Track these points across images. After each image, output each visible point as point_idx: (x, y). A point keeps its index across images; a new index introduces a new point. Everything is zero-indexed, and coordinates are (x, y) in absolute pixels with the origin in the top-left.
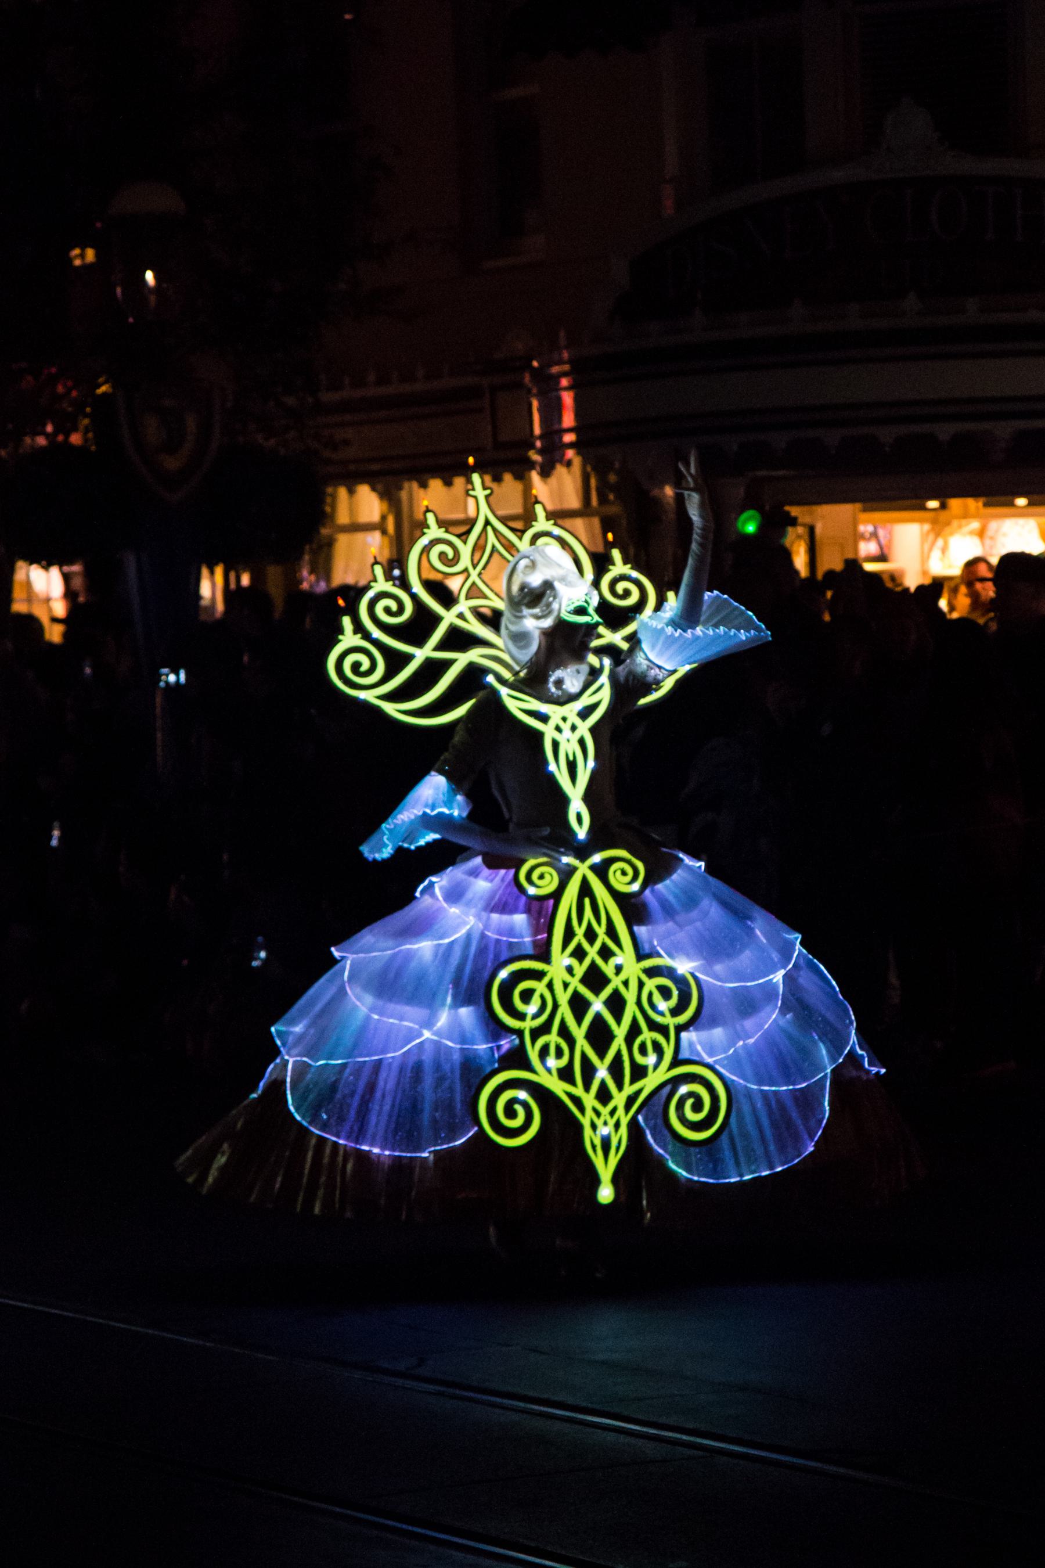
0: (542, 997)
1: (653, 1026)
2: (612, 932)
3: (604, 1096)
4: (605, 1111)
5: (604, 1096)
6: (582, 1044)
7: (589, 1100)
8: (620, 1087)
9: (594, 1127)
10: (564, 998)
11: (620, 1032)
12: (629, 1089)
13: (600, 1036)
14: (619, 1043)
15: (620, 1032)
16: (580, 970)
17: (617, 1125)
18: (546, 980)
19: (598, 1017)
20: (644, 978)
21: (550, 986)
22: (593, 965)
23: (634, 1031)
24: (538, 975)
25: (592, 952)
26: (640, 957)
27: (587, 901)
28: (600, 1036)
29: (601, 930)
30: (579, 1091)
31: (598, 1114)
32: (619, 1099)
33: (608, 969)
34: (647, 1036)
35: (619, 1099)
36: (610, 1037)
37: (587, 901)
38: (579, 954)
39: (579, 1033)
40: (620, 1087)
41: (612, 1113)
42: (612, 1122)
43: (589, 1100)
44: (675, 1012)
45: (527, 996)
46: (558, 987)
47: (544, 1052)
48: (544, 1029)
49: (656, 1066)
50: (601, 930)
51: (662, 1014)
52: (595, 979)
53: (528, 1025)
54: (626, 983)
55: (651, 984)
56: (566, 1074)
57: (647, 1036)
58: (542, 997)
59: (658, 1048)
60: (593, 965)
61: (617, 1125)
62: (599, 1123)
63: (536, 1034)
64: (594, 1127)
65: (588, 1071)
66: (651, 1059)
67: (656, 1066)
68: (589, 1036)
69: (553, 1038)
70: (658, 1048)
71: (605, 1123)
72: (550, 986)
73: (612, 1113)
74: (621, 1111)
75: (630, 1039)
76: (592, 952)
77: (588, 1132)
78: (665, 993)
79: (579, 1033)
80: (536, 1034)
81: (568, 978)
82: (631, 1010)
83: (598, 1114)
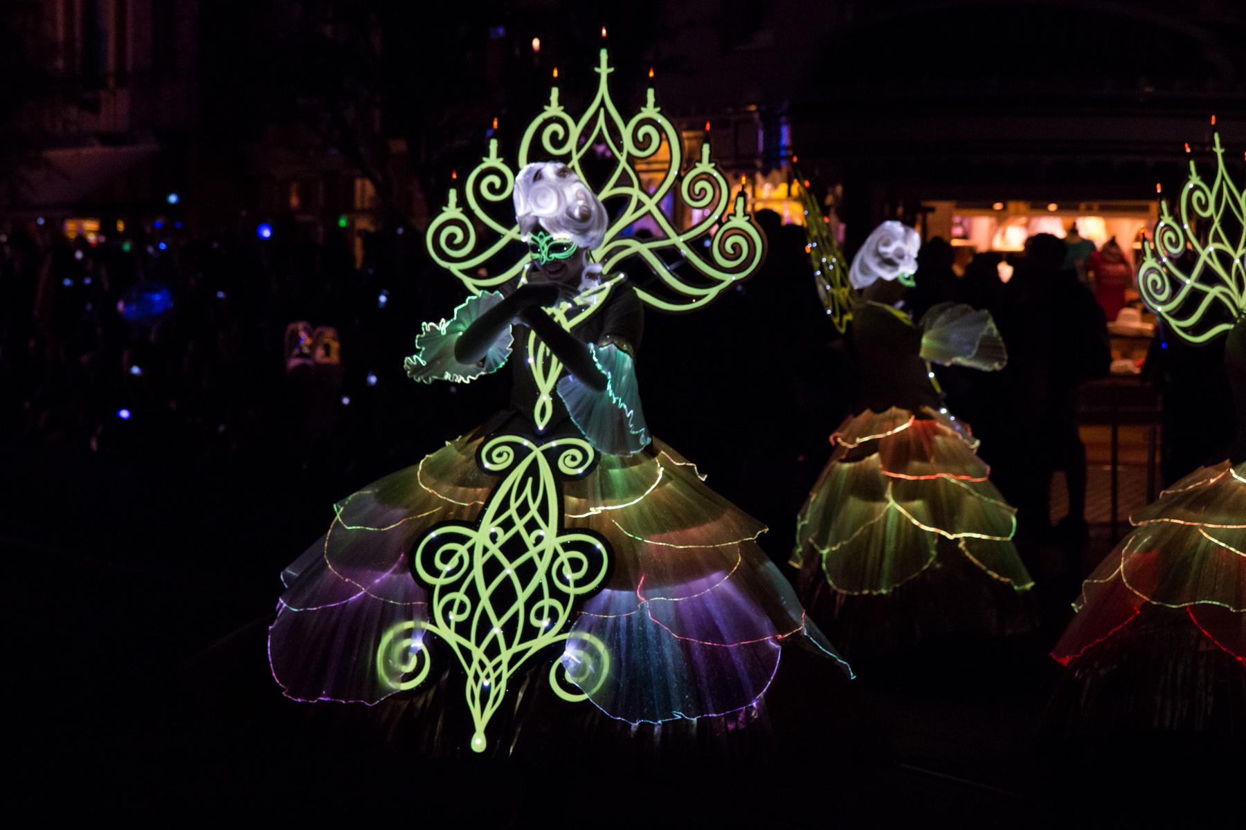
0: (461, 559)
1: (555, 594)
2: (544, 510)
3: (493, 651)
4: (490, 665)
5: (493, 651)
6: (485, 603)
7: (478, 654)
8: (509, 646)
9: (477, 678)
10: (479, 561)
11: (523, 596)
12: (516, 648)
13: (503, 598)
14: (519, 605)
15: (523, 596)
16: (503, 538)
17: (498, 679)
18: (469, 544)
19: (508, 579)
20: (560, 550)
21: (471, 551)
22: (518, 534)
23: (537, 595)
24: (462, 539)
25: (520, 525)
26: (561, 531)
27: (530, 480)
28: (503, 598)
29: (534, 507)
30: (470, 645)
31: (483, 666)
32: (505, 655)
33: (529, 540)
34: (547, 602)
35: (505, 655)
36: (514, 598)
37: (530, 480)
38: (507, 525)
39: (485, 593)
40: (509, 646)
41: (495, 668)
42: (493, 676)
43: (478, 654)
44: (578, 583)
45: (446, 557)
46: (478, 551)
47: (448, 607)
48: (455, 587)
49: (547, 631)
50: (534, 507)
51: (566, 583)
52: (514, 547)
53: (439, 582)
54: (541, 554)
55: (564, 556)
56: (463, 629)
57: (547, 602)
58: (461, 559)
59: (554, 614)
60: (518, 534)
61: (498, 679)
62: (482, 675)
63: (445, 590)
64: (477, 678)
65: (485, 625)
66: (545, 622)
67: (547, 631)
68: (493, 599)
69: (460, 596)
70: (554, 614)
71: (488, 676)
72: (471, 551)
73: (495, 668)
74: (504, 667)
75: (529, 604)
76: (520, 525)
77: (470, 682)
78: (575, 565)
79: (485, 593)
80: (445, 590)
81: (489, 544)
82: (539, 577)
83: (483, 666)
